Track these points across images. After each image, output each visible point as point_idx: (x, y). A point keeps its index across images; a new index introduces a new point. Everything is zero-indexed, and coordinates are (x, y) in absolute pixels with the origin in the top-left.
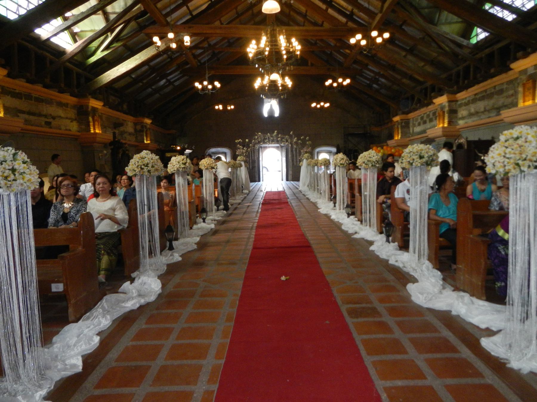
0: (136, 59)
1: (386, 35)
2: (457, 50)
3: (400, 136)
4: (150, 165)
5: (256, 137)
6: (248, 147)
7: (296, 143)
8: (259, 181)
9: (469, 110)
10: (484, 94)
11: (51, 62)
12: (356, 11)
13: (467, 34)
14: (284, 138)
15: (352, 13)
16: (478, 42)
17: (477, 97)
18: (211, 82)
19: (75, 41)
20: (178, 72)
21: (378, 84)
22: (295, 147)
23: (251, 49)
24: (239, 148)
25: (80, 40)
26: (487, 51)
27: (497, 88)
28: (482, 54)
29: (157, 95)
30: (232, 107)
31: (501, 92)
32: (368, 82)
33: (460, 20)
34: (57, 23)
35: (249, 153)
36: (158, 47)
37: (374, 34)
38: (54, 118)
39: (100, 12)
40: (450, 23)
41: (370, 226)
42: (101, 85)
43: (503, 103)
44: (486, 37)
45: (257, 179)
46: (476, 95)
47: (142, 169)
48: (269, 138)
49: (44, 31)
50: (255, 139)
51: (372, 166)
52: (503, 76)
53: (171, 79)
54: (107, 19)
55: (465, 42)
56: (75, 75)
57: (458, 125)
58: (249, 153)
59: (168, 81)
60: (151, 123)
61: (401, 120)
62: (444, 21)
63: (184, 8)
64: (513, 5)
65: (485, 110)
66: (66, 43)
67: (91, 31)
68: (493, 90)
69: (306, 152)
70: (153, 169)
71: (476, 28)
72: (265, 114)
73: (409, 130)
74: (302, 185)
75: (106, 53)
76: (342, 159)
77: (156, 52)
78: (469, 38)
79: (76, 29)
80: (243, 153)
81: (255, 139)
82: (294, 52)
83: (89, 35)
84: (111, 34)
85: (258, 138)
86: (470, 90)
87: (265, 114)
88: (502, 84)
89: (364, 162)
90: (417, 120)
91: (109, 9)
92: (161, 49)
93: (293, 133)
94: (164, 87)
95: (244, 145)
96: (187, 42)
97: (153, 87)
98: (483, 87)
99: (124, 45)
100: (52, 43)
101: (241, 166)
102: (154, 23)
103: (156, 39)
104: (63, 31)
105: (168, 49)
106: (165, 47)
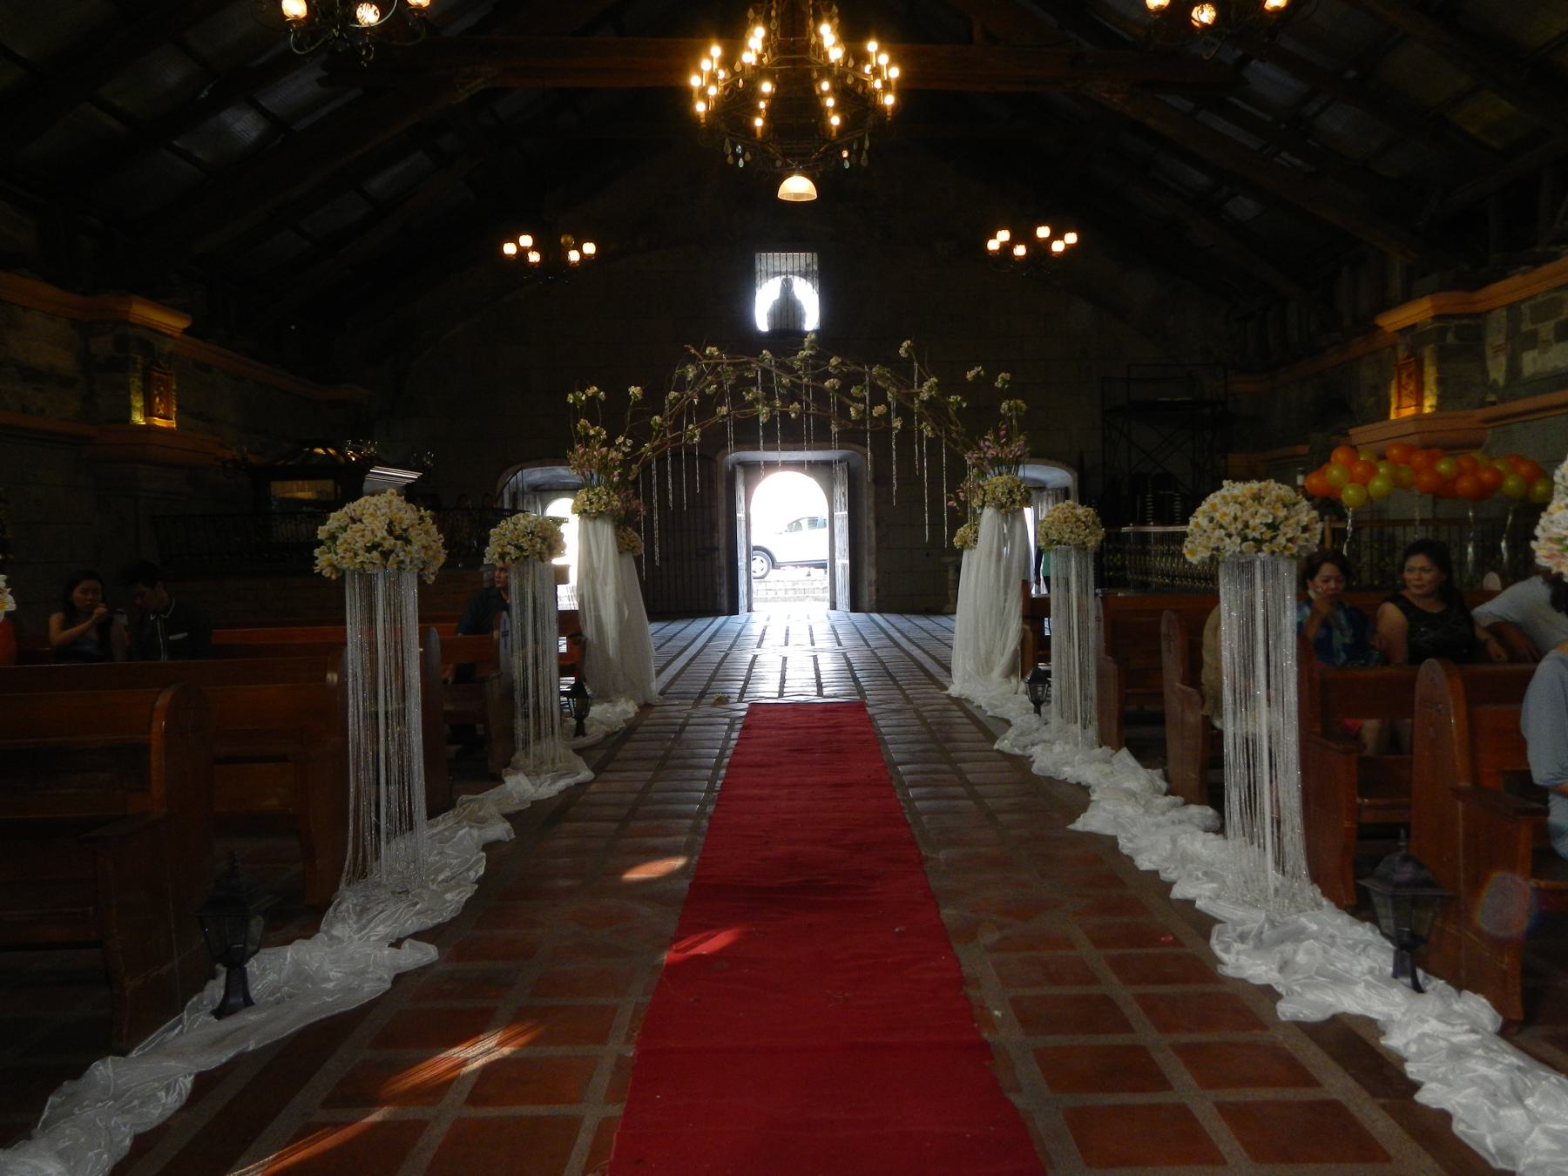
5: (691, 372)
6: (641, 433)
7: (935, 408)
8: (734, 610)
14: (857, 379)
22: (928, 432)
23: (706, 76)
24: (587, 440)
30: (589, 248)
35: (646, 467)
48: (766, 373)
50: (681, 385)
58: (646, 467)
61: (1436, 318)
73: (1485, 372)
85: (700, 376)
87: (762, 323)
93: (915, 349)
95: (613, 416)
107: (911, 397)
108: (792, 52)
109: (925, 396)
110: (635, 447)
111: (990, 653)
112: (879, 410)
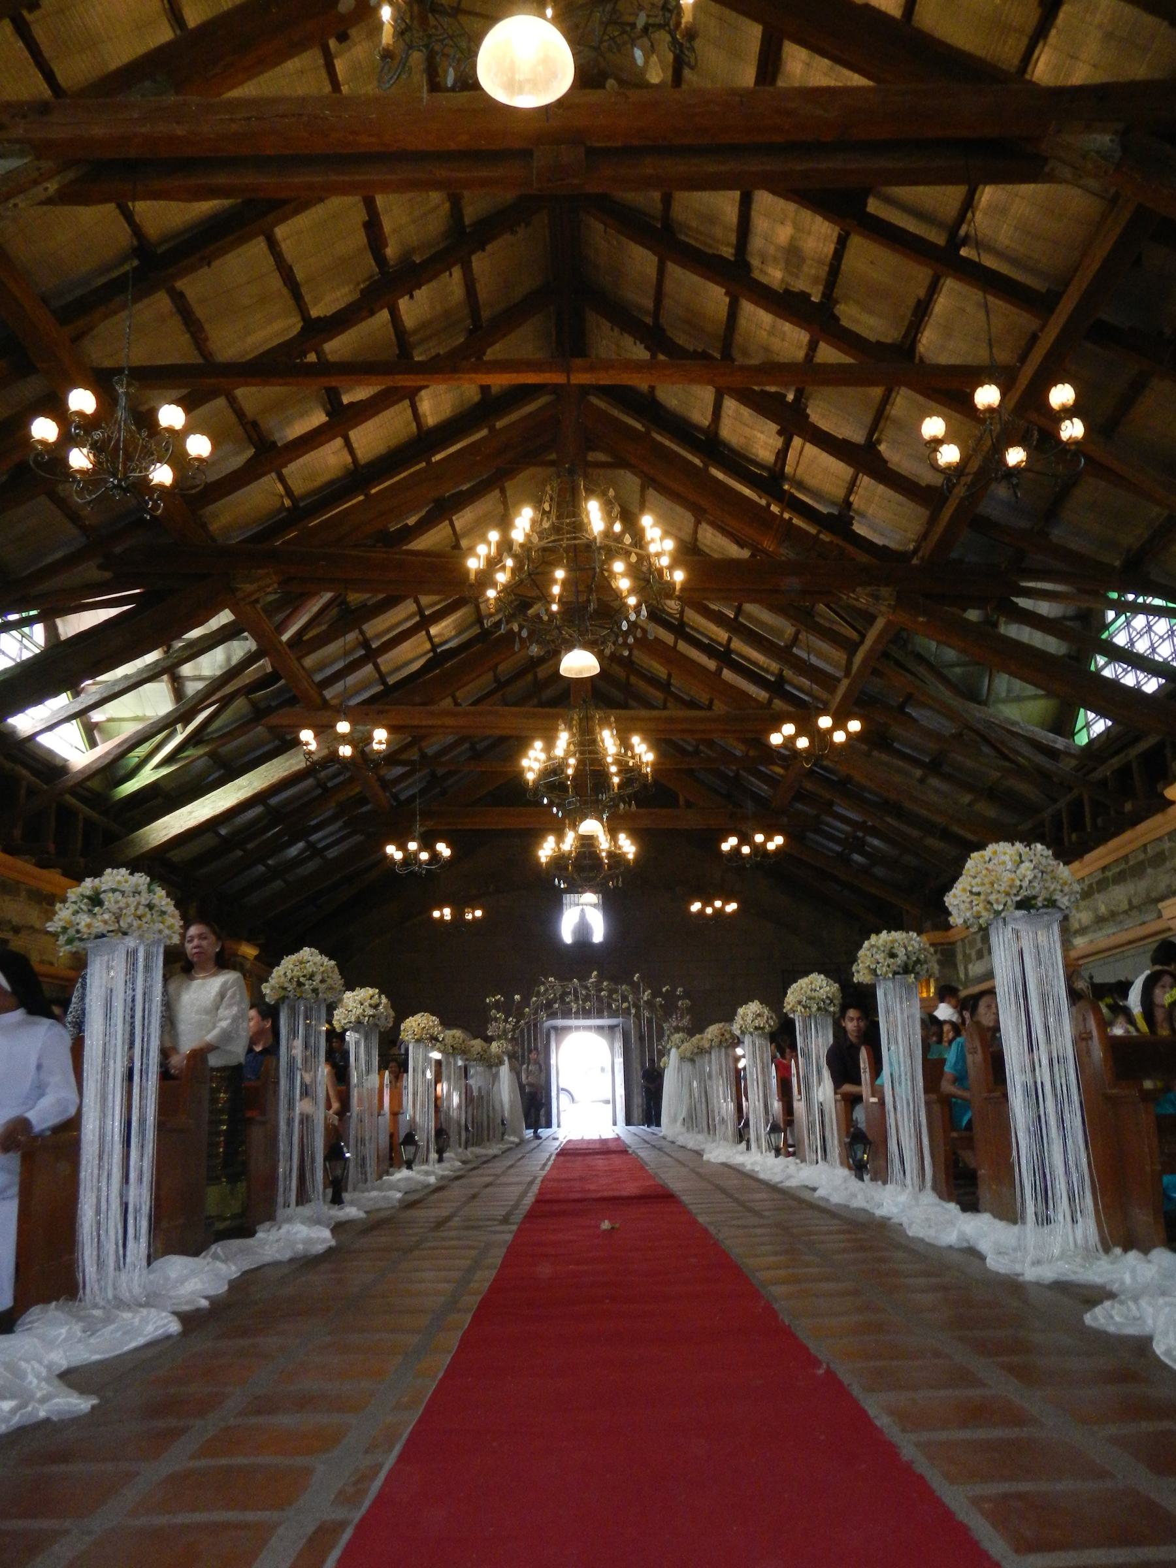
0: (240, 788)
1: (855, 726)
2: (1041, 759)
3: (932, 990)
4: (318, 978)
5: (542, 989)
6: (520, 1016)
7: (650, 1004)
9: (1096, 910)
10: (1123, 866)
11: (32, 792)
12: (788, 673)
13: (1064, 725)
14: (616, 991)
15: (780, 678)
16: (1091, 742)
17: (1109, 874)
18: (427, 845)
19: (93, 744)
20: (339, 824)
21: (862, 853)
24: (496, 1019)
25: (104, 741)
26: (1116, 762)
27: (1150, 851)
28: (1104, 771)
29: (278, 884)
30: (478, 913)
31: (1159, 860)
32: (838, 849)
33: (1043, 692)
34: (61, 702)
35: (522, 1031)
36: (310, 753)
37: (825, 722)
38: (16, 930)
39: (165, 677)
40: (1019, 699)
41: (825, 1157)
42: (145, 849)
43: (1169, 886)
44: (1108, 729)
45: (543, 1120)
46: (1104, 869)
47: (300, 984)
49: (24, 722)
50: (538, 994)
51: (819, 1009)
52: (1158, 819)
53: (320, 840)
54: (178, 692)
55: (1060, 743)
56: (81, 825)
57: (1074, 948)
59: (311, 846)
60: (256, 958)
62: (1003, 695)
63: (369, 668)
64: (1157, 658)
65: (1132, 907)
66: (71, 748)
67: (136, 719)
68: (1142, 857)
69: (677, 1030)
70: (324, 986)
71: (1082, 710)
72: (567, 935)
73: (958, 973)
74: (670, 1125)
75: (164, 771)
76: (759, 1015)
77: (303, 765)
78: (1072, 734)
79: (97, 716)
80: (505, 1032)
81: (538, 994)
82: (638, 768)
83: (129, 730)
84: (185, 727)
85: (546, 990)
86: (1088, 857)
87: (567, 935)
88: (1160, 839)
89: (800, 1002)
90: (972, 943)
91: (186, 670)
92: (315, 757)
94: (298, 861)
95: (507, 1008)
96: (380, 743)
97: (270, 862)
98: (1117, 849)
99: (212, 755)
100: (40, 746)
101: (501, 1063)
102: (293, 701)
103: (307, 735)
104: (68, 719)
105: (333, 757)
106: (325, 752)
107: (639, 999)
108: (587, 746)
109: (645, 998)
110: (518, 1022)
111: (675, 1115)
112: (625, 1005)
